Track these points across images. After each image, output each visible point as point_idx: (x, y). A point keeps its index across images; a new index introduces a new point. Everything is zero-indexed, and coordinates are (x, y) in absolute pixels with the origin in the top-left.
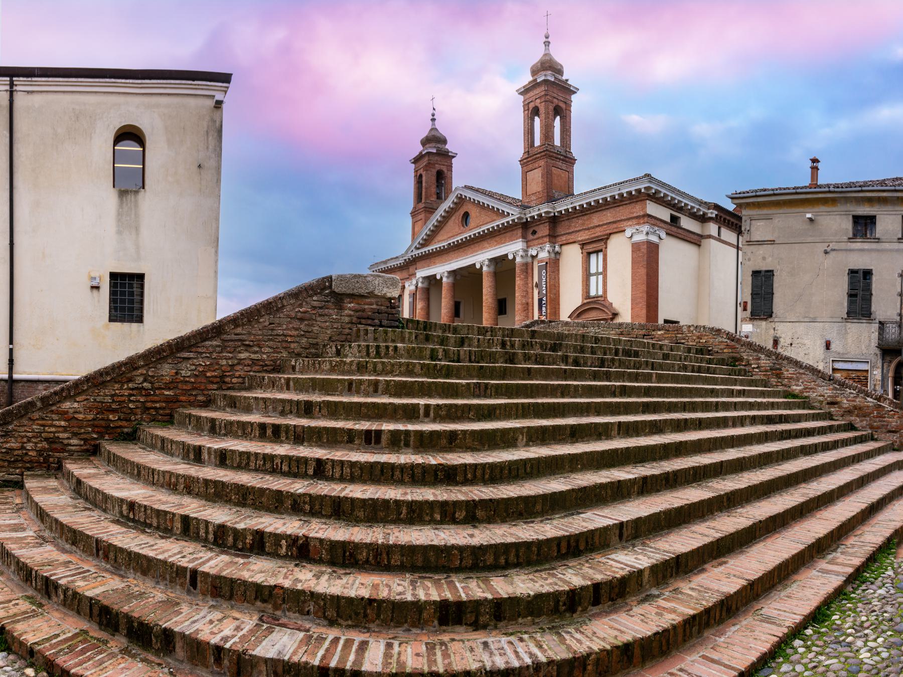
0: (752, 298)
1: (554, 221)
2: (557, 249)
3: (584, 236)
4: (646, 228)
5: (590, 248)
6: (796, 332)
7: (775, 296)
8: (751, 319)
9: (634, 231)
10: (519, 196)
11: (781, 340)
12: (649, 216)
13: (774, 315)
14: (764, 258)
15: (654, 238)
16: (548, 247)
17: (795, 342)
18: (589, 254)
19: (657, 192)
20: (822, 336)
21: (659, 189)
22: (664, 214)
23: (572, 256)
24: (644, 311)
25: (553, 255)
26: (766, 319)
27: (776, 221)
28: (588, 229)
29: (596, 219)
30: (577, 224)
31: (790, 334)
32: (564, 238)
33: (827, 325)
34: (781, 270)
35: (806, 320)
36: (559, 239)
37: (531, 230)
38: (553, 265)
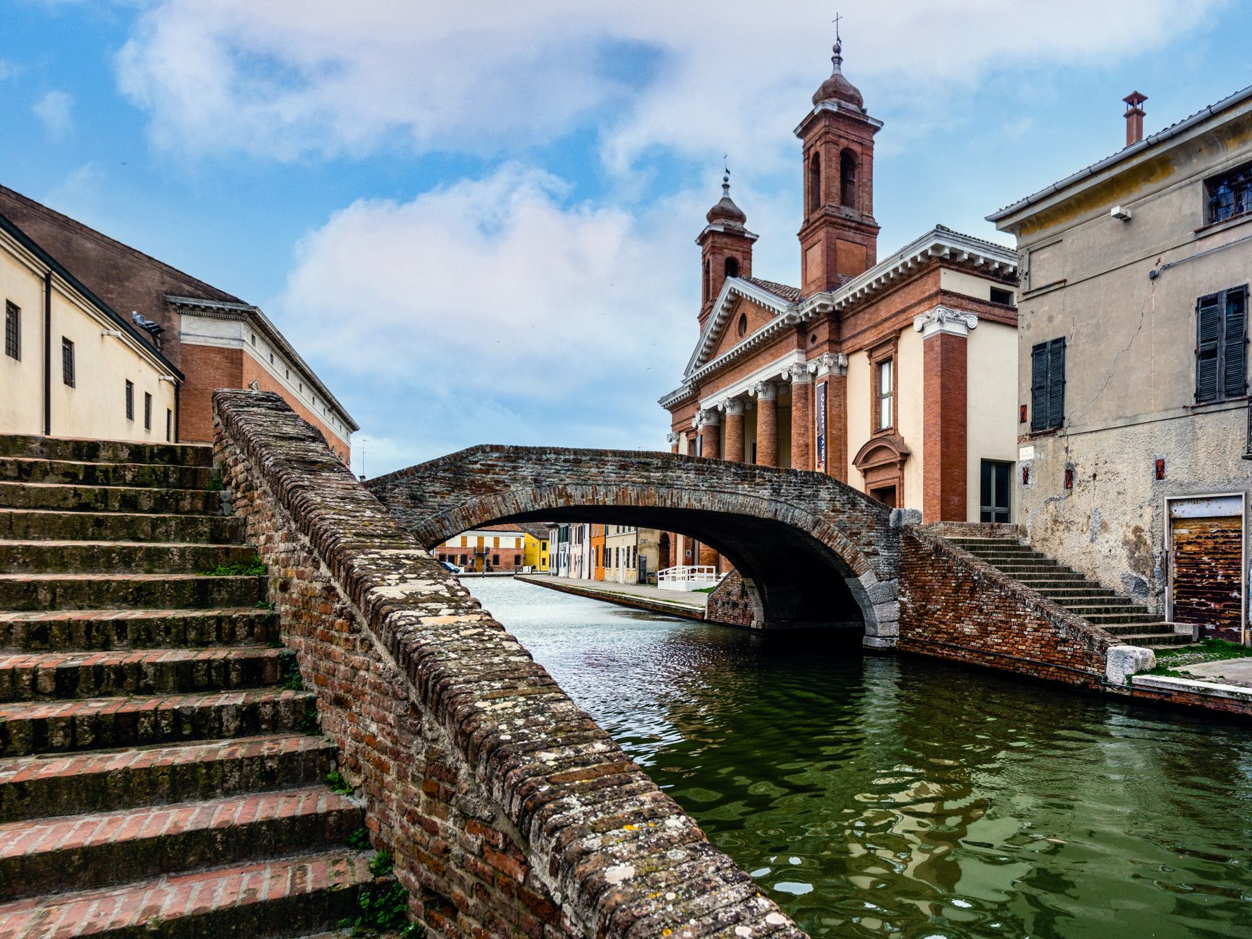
0: (1034, 397)
1: (837, 318)
2: (841, 361)
5: (879, 355)
6: (1102, 451)
7: (1067, 386)
8: (1032, 436)
11: (1078, 469)
13: (1066, 423)
14: (1051, 319)
16: (826, 358)
17: (1102, 469)
18: (880, 365)
20: (1149, 452)
23: (860, 367)
24: (939, 447)
25: (836, 371)
26: (1053, 433)
27: (1067, 243)
28: (875, 326)
30: (863, 320)
31: (1092, 455)
32: (849, 344)
33: (1157, 427)
34: (1078, 333)
35: (1119, 423)
36: (844, 346)
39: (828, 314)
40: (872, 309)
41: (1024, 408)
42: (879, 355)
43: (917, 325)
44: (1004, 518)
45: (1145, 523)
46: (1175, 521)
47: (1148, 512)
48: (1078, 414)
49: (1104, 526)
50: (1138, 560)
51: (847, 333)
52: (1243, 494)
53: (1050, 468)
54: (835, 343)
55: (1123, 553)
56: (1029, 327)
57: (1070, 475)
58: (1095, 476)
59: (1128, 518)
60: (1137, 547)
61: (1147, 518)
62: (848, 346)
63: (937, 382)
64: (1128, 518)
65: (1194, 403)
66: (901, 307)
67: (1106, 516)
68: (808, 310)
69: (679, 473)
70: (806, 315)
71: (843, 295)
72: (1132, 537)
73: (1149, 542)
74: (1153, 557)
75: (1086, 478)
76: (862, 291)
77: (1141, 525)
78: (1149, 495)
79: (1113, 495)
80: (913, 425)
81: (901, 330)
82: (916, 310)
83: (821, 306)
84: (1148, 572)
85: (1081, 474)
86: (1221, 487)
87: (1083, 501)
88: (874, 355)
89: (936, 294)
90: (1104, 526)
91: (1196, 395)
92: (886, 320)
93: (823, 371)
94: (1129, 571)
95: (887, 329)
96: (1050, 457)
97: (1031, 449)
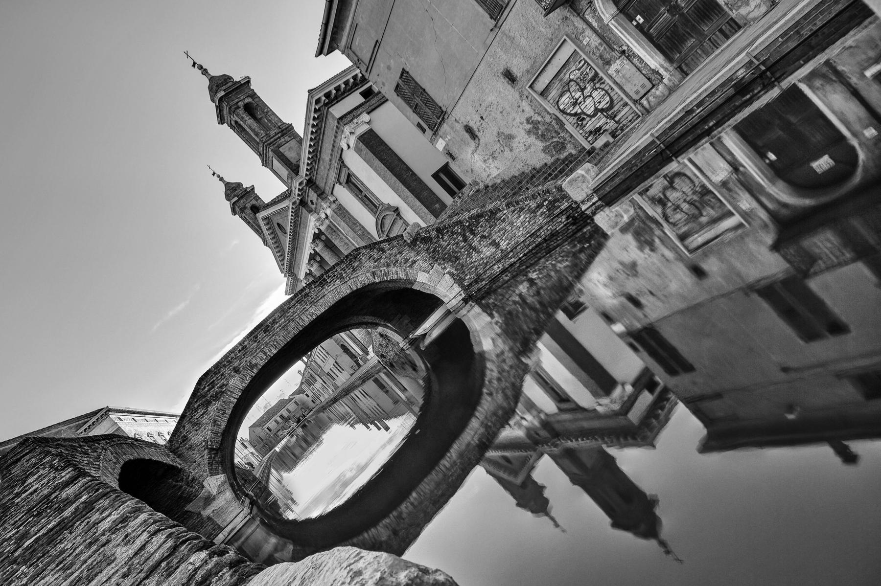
0: (418, 114)
3: (333, 175)
4: (347, 130)
9: (345, 140)
10: (283, 188)
11: (471, 124)
12: (341, 118)
13: (444, 109)
14: (389, 68)
15: (364, 129)
17: (482, 110)
19: (338, 89)
21: (327, 91)
22: (355, 99)
27: (362, 21)
29: (326, 156)
31: (471, 109)
34: (407, 59)
36: (327, 192)
37: (309, 203)
38: (341, 211)
39: (307, 185)
40: (321, 162)
41: (419, 125)
42: (343, 178)
43: (345, 147)
44: (460, 185)
45: (529, 112)
46: (543, 94)
47: (525, 104)
48: (445, 97)
49: (510, 137)
50: (543, 135)
51: (321, 185)
52: (565, 37)
53: (457, 139)
54: (322, 194)
55: (532, 139)
56: (383, 84)
57: (469, 130)
58: (482, 118)
59: (518, 120)
60: (537, 129)
61: (527, 108)
62: (328, 190)
63: (377, 162)
64: (518, 120)
65: (494, 23)
66: (331, 147)
67: (507, 132)
68: (297, 192)
69: (291, 311)
70: (299, 195)
71: (303, 170)
72: (529, 126)
73: (540, 119)
74: (550, 124)
75: (479, 124)
76: (309, 158)
77: (527, 115)
78: (517, 95)
79: (499, 116)
80: (385, 191)
81: (341, 157)
82: (338, 141)
83: (300, 184)
84: (554, 135)
85: (474, 125)
86: (549, 48)
87: (487, 136)
88: (341, 181)
89: (338, 123)
90: (510, 137)
91: (491, 18)
92: (331, 160)
93: (329, 212)
94: (543, 144)
95: (335, 164)
96: (452, 133)
97: (441, 140)
